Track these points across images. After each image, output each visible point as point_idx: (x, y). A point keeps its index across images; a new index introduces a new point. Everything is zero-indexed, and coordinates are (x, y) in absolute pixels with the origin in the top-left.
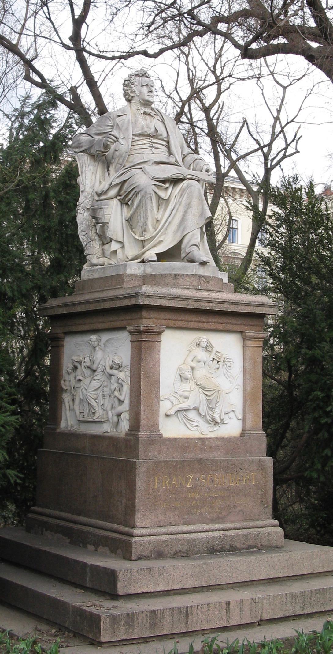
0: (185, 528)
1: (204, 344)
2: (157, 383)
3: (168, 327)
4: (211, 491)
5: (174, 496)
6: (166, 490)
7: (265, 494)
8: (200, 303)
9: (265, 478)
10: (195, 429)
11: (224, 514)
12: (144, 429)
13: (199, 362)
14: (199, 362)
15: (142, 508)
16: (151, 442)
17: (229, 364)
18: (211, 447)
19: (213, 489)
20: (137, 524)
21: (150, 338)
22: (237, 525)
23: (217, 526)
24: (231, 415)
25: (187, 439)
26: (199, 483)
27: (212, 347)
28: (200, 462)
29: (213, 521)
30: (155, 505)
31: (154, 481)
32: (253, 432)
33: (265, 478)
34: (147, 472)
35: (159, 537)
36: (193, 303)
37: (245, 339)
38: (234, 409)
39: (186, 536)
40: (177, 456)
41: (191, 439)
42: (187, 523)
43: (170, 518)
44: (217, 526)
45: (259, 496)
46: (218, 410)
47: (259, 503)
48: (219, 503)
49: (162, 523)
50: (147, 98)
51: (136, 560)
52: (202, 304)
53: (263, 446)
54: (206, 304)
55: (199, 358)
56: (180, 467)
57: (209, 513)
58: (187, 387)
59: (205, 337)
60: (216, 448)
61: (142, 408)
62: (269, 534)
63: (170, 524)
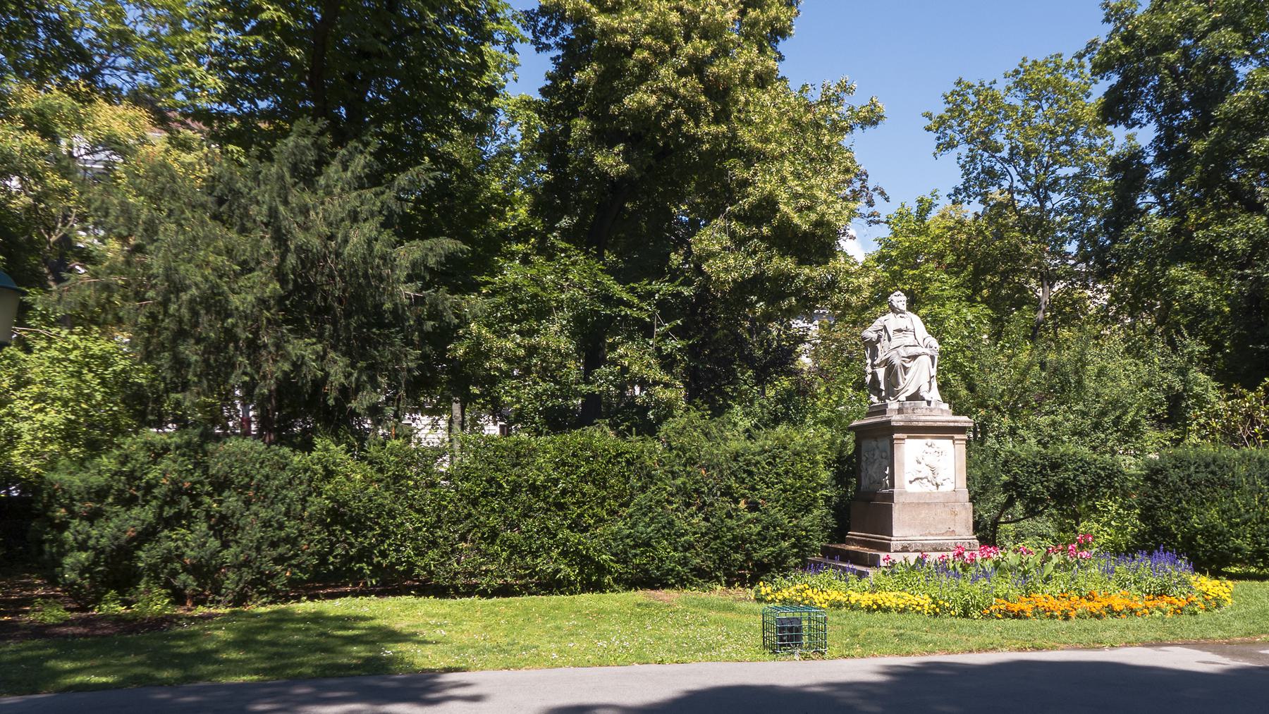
2: (903, 464)
3: (908, 437)
16: (901, 494)
28: (928, 504)
29: (936, 535)
40: (915, 501)
48: (940, 526)
59: (929, 441)
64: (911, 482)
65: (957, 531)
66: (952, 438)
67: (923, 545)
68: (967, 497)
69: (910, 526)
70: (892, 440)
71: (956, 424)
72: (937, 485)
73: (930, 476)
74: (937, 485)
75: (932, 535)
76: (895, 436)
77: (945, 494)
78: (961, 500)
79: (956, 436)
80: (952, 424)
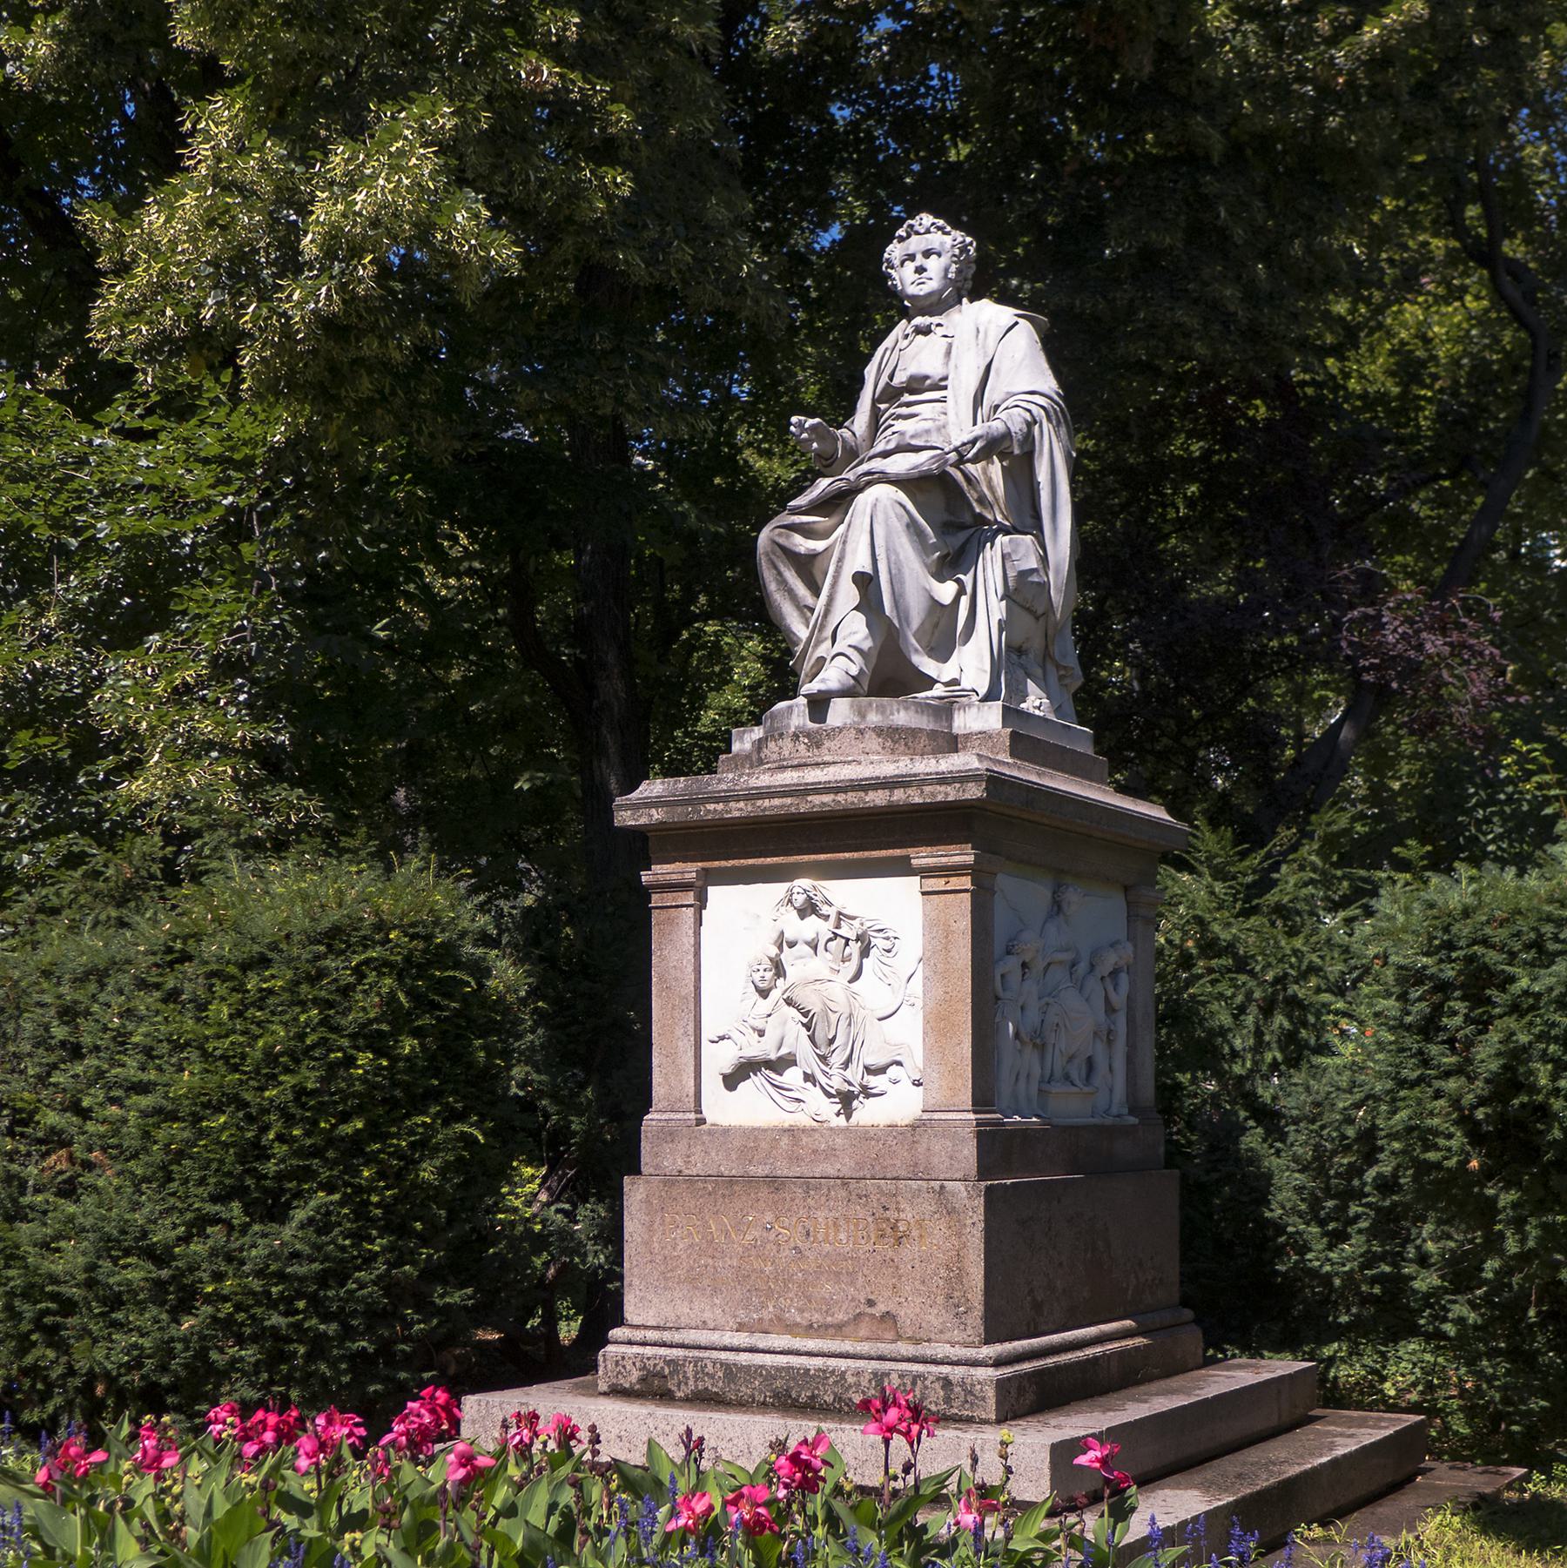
0: (729, 1338)
1: (800, 900)
4: (803, 1256)
5: (710, 1261)
6: (691, 1246)
7: (959, 1277)
8: (759, 803)
9: (959, 1235)
10: (793, 1106)
11: (841, 1317)
12: (660, 1106)
13: (792, 945)
14: (792, 945)
15: (636, 1282)
16: (669, 1134)
17: (887, 944)
18: (815, 1152)
19: (807, 1253)
20: (627, 1315)
21: (669, 899)
22: (864, 1348)
23: (811, 1344)
24: (893, 1071)
25: (754, 1129)
26: (772, 1236)
27: (831, 905)
28: (774, 1182)
29: (810, 1330)
30: (666, 1279)
31: (663, 1223)
32: (936, 1116)
33: (959, 1235)
34: (647, 1201)
35: (662, 1351)
36: (742, 804)
37: (926, 872)
38: (898, 1058)
39: (723, 1355)
41: (765, 1130)
42: (740, 1328)
43: (703, 1311)
44: (811, 1344)
45: (941, 1282)
46: (837, 1059)
47: (940, 1300)
48: (827, 1288)
49: (684, 1321)
50: (912, 290)
51: (605, 1394)
52: (767, 803)
53: (966, 1152)
54: (776, 802)
55: (789, 936)
56: (724, 1196)
57: (801, 1311)
58: (765, 1005)
60: (831, 1153)
61: (655, 1061)
62: (947, 1383)
63: (704, 1325)
64: (732, 1081)
65: (906, 1314)
66: (902, 868)
67: (730, 1371)
68: (968, 1152)
69: (693, 1281)
70: (644, 893)
71: (899, 796)
72: (846, 1100)
73: (805, 1051)
74: (846, 1100)
75: (790, 1329)
76: (659, 872)
77: (867, 1135)
78: (940, 1163)
79: (923, 857)
80: (878, 798)
